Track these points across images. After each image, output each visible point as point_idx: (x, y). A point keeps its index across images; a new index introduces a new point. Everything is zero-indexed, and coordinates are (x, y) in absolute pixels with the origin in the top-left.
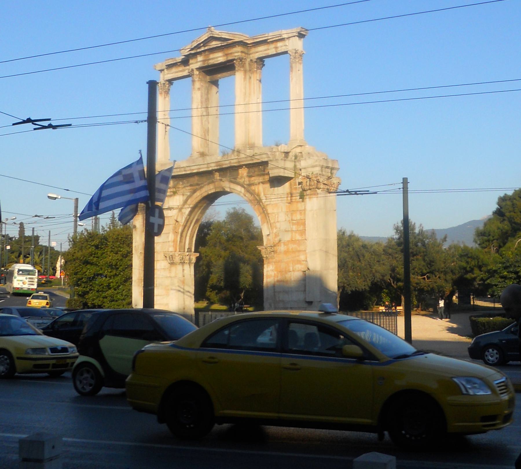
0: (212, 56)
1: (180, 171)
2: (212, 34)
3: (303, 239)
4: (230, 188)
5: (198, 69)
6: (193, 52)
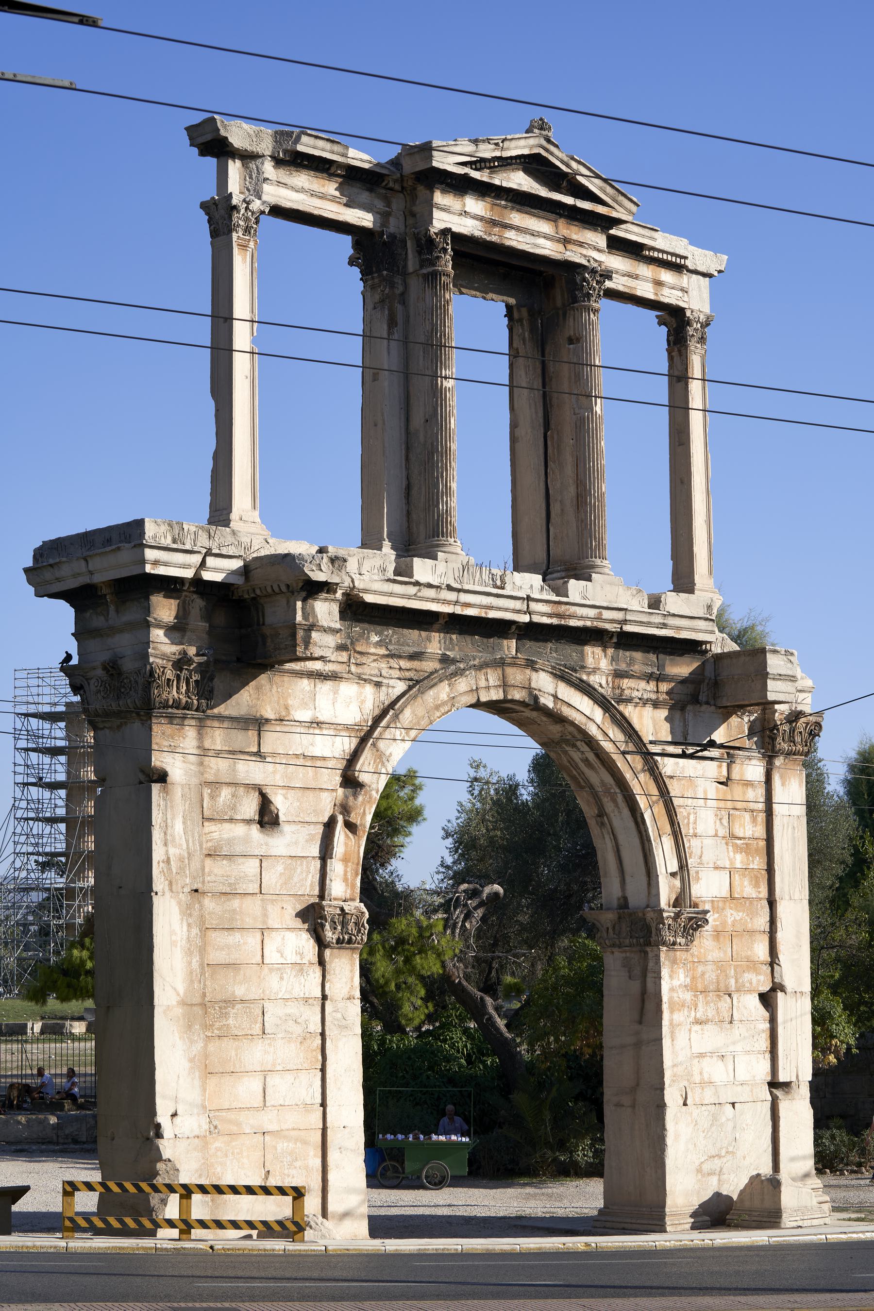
0: (516, 218)
1: (415, 597)
2: (547, 150)
3: (761, 896)
4: (555, 697)
5: (458, 238)
6: (476, 175)
